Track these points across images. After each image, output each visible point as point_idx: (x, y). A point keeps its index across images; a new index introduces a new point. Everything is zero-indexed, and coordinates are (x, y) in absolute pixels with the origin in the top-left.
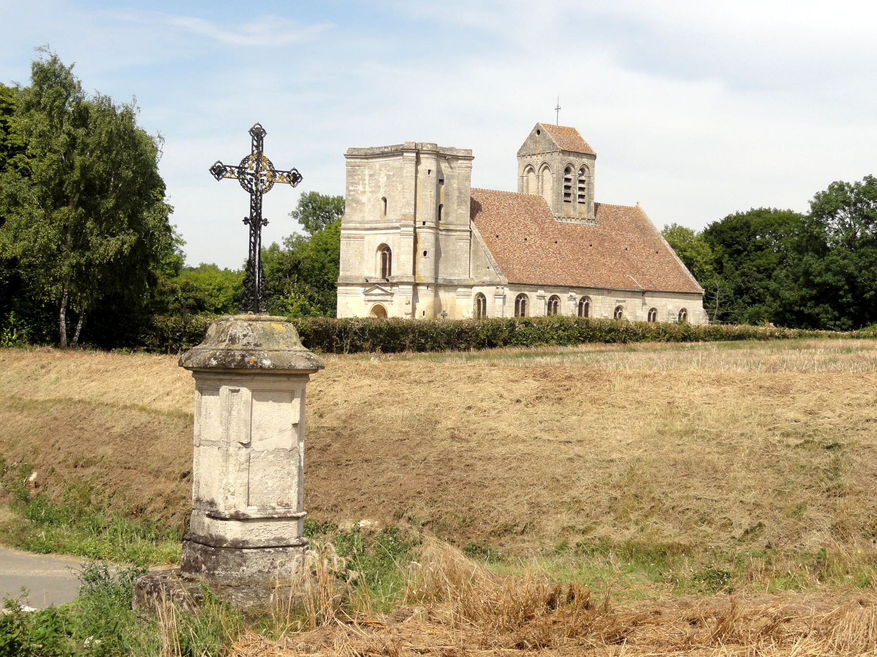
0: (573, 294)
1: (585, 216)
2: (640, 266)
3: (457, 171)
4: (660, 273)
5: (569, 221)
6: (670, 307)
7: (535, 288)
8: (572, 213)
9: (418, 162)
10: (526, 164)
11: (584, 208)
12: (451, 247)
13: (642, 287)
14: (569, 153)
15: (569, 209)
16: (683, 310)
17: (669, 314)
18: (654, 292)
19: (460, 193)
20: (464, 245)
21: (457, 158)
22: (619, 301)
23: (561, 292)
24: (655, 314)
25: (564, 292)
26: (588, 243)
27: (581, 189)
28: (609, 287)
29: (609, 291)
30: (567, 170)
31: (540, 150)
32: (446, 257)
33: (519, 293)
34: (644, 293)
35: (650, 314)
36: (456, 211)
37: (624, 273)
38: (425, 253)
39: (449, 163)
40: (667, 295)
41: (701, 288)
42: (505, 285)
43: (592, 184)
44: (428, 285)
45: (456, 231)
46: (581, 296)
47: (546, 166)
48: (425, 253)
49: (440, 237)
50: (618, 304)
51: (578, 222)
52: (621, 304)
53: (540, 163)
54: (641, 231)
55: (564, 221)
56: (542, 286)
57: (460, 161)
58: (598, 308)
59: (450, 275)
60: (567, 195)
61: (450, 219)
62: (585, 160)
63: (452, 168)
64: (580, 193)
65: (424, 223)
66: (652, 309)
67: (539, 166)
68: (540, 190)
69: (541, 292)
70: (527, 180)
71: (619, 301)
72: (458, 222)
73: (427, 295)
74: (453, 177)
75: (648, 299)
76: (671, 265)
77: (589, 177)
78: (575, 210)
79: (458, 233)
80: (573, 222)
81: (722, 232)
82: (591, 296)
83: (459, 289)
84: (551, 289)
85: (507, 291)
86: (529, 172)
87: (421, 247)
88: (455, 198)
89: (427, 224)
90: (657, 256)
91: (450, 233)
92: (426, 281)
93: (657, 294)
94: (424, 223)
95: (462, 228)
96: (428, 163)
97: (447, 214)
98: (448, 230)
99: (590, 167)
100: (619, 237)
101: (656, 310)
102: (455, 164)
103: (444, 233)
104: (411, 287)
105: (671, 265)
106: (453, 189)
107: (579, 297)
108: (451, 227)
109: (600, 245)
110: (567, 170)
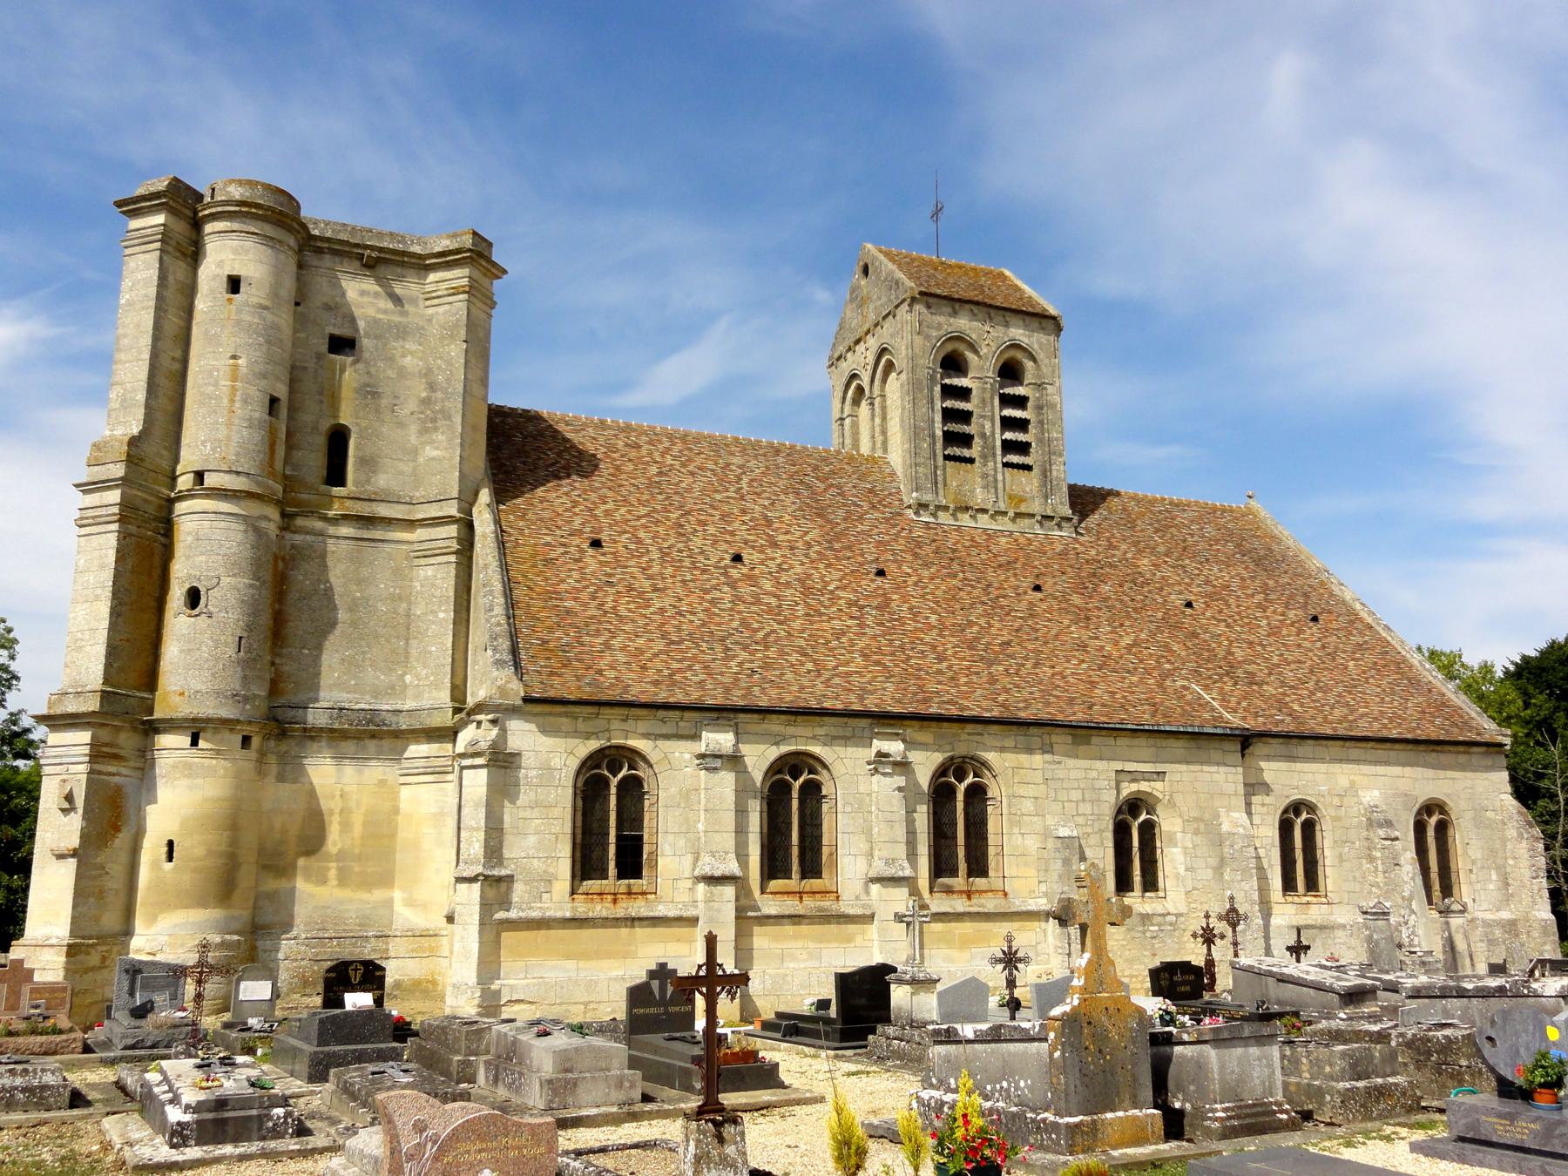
0: (895, 747)
1: (1036, 507)
2: (1239, 654)
3: (417, 313)
4: (1325, 678)
5: (965, 520)
6: (1371, 796)
7: (687, 721)
8: (980, 497)
9: (185, 249)
10: (844, 380)
11: (1028, 484)
12: (384, 585)
13: (1235, 720)
14: (956, 303)
15: (972, 483)
16: (1429, 808)
17: (1371, 824)
18: (1297, 741)
19: (432, 387)
20: (438, 577)
21: (421, 264)
22: (1135, 777)
23: (830, 740)
24: (1309, 827)
25: (846, 740)
26: (1026, 584)
27: (1008, 423)
28: (1079, 716)
29: (1085, 734)
30: (953, 363)
31: (872, 317)
32: (354, 624)
33: (594, 745)
34: (1246, 741)
35: (1285, 828)
36: (415, 452)
37: (1169, 674)
38: (194, 598)
39: (380, 281)
40: (1355, 751)
41: (1494, 726)
42: (513, 711)
43: (1053, 406)
44: (196, 730)
45: (411, 524)
46: (938, 758)
47: (884, 363)
48: (194, 598)
49: (331, 545)
50: (1129, 789)
51: (1004, 524)
52: (1144, 786)
53: (871, 359)
54: (1258, 562)
55: (944, 518)
56: (722, 714)
57: (433, 277)
58: (1028, 806)
59: (376, 694)
60: (966, 440)
61: (382, 481)
62: (1018, 333)
63: (397, 300)
64: (1009, 435)
65: (199, 476)
66: (1296, 807)
67: (869, 372)
68: (879, 439)
69: (720, 739)
70: (855, 426)
71: (1135, 777)
72: (418, 494)
73: (188, 770)
74: (402, 332)
75: (1273, 770)
76: (1370, 658)
77: (1040, 386)
78: (991, 484)
79: (421, 533)
80: (984, 521)
81: (1543, 670)
82: (991, 757)
83: (417, 750)
84: (775, 725)
85: (523, 736)
86: (856, 402)
87: (182, 573)
88: (412, 405)
89: (210, 480)
90: (1313, 630)
91: (377, 534)
92: (184, 709)
93: (1308, 748)
94: (199, 476)
95: (434, 511)
96: (228, 251)
97: (369, 464)
98: (369, 521)
99: (1041, 356)
100: (1168, 572)
101: (1312, 808)
102: (408, 287)
103: (346, 530)
104: (85, 736)
105: (1370, 658)
106: (402, 373)
107: (925, 764)
108: (383, 511)
109: (1080, 588)
110: (953, 363)
